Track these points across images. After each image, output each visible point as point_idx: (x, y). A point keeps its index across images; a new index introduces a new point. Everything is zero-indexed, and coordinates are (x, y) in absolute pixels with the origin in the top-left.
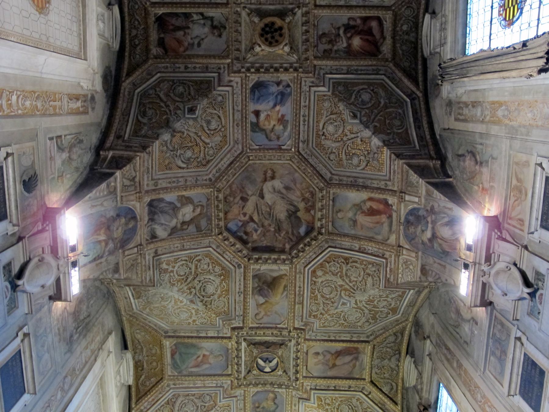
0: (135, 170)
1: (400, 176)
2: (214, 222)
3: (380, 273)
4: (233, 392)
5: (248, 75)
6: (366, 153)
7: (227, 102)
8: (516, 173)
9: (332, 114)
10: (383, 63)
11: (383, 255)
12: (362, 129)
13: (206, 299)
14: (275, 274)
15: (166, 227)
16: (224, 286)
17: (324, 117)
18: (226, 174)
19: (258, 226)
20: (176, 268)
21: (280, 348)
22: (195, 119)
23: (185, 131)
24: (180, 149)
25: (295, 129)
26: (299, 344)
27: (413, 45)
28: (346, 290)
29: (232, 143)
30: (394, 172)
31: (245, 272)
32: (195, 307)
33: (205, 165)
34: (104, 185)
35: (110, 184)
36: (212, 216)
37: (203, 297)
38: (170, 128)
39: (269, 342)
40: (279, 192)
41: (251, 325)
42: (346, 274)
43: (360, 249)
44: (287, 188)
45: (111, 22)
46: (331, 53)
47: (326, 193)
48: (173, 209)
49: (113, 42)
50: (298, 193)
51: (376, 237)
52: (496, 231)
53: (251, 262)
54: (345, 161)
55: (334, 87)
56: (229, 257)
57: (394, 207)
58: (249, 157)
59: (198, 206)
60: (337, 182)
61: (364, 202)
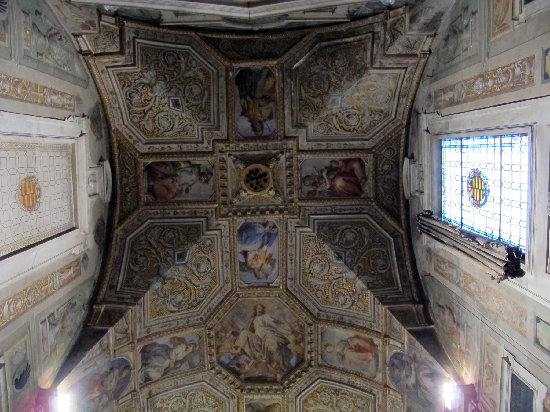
0: (127, 323)
1: (384, 320)
2: (207, 358)
3: (369, 407)
5: (235, 218)
6: (351, 293)
7: (216, 245)
8: (487, 353)
9: (318, 253)
10: (366, 203)
11: (371, 391)
12: (347, 270)
14: (268, 404)
15: (159, 368)
17: (310, 256)
18: (217, 313)
19: (250, 359)
20: (170, 405)
22: (185, 265)
23: (176, 277)
24: (171, 294)
25: (283, 267)
27: (394, 184)
29: (221, 283)
30: (378, 315)
31: (238, 402)
33: (196, 306)
34: (97, 346)
35: (103, 342)
36: (204, 352)
38: (161, 276)
40: (270, 326)
42: (337, 405)
43: (349, 382)
44: (277, 322)
45: (102, 178)
46: (315, 194)
47: (315, 328)
48: (166, 351)
49: (104, 195)
50: (288, 327)
51: (364, 373)
52: (472, 401)
53: (243, 393)
54: (331, 299)
55: (319, 226)
56: (223, 389)
57: (379, 348)
58: (238, 295)
59: (190, 345)
60: (325, 318)
61: (351, 338)
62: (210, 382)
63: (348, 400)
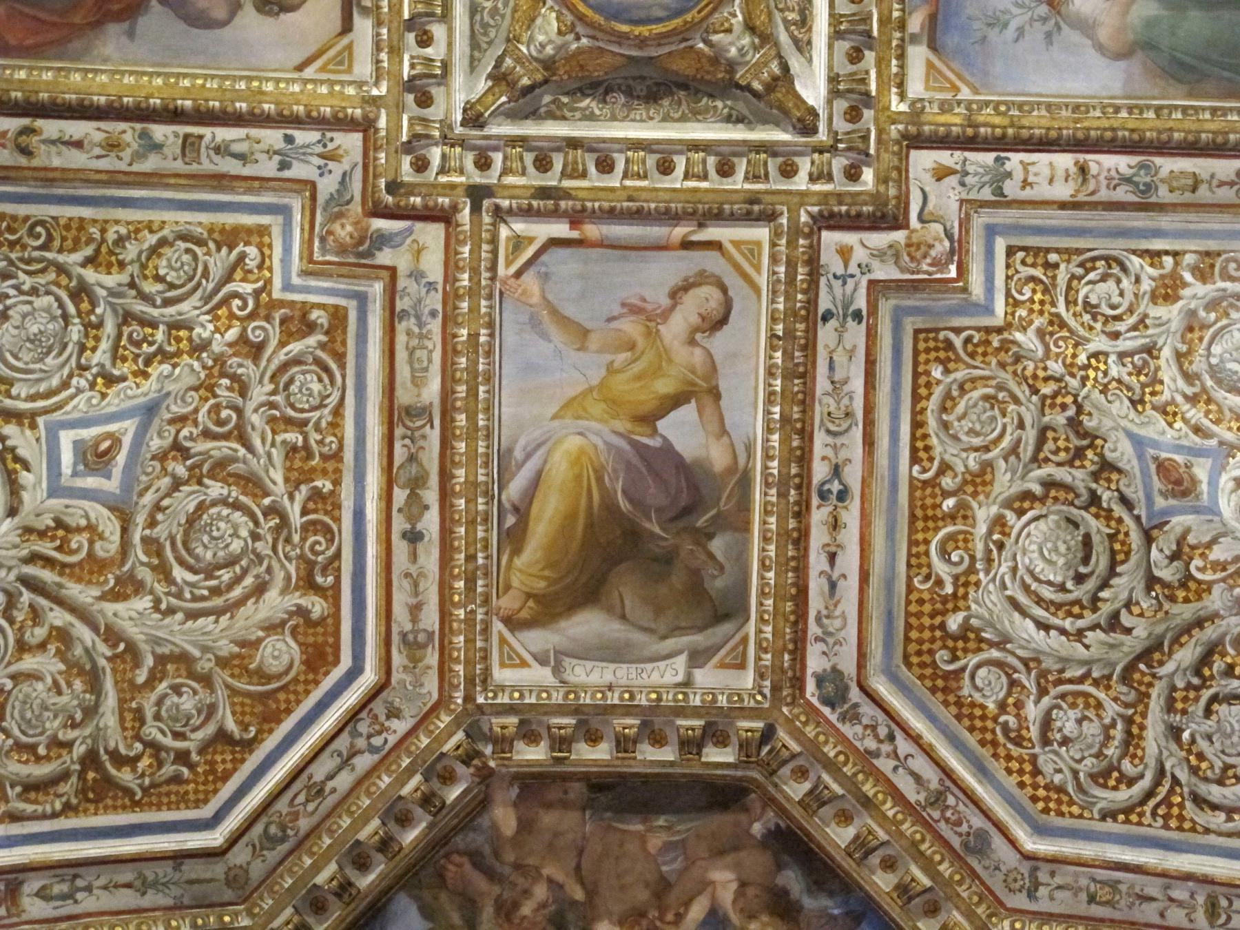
13: (1077, 477)
16: (944, 554)
21: (548, 65)
26: (410, 85)
28: (94, 566)
32: (1155, 428)
37: (1094, 499)
39: (629, 93)
41: (762, 233)
42: (94, 682)
53: (759, 725)
56: (901, 762)
62: (982, 835)
63: (19, 747)
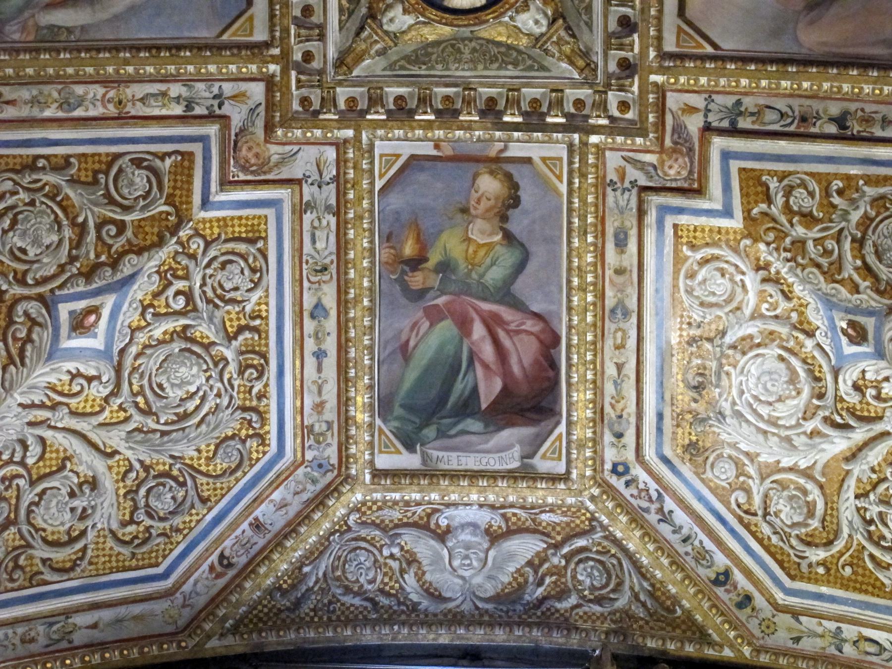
4: (274, 151)
